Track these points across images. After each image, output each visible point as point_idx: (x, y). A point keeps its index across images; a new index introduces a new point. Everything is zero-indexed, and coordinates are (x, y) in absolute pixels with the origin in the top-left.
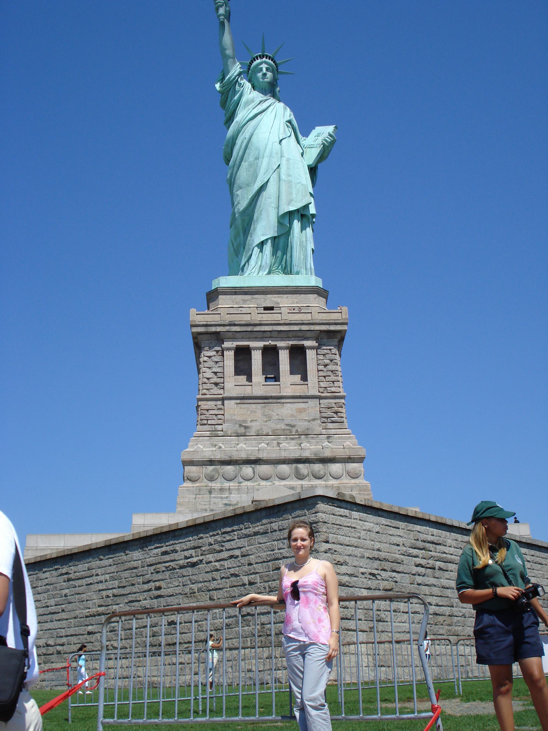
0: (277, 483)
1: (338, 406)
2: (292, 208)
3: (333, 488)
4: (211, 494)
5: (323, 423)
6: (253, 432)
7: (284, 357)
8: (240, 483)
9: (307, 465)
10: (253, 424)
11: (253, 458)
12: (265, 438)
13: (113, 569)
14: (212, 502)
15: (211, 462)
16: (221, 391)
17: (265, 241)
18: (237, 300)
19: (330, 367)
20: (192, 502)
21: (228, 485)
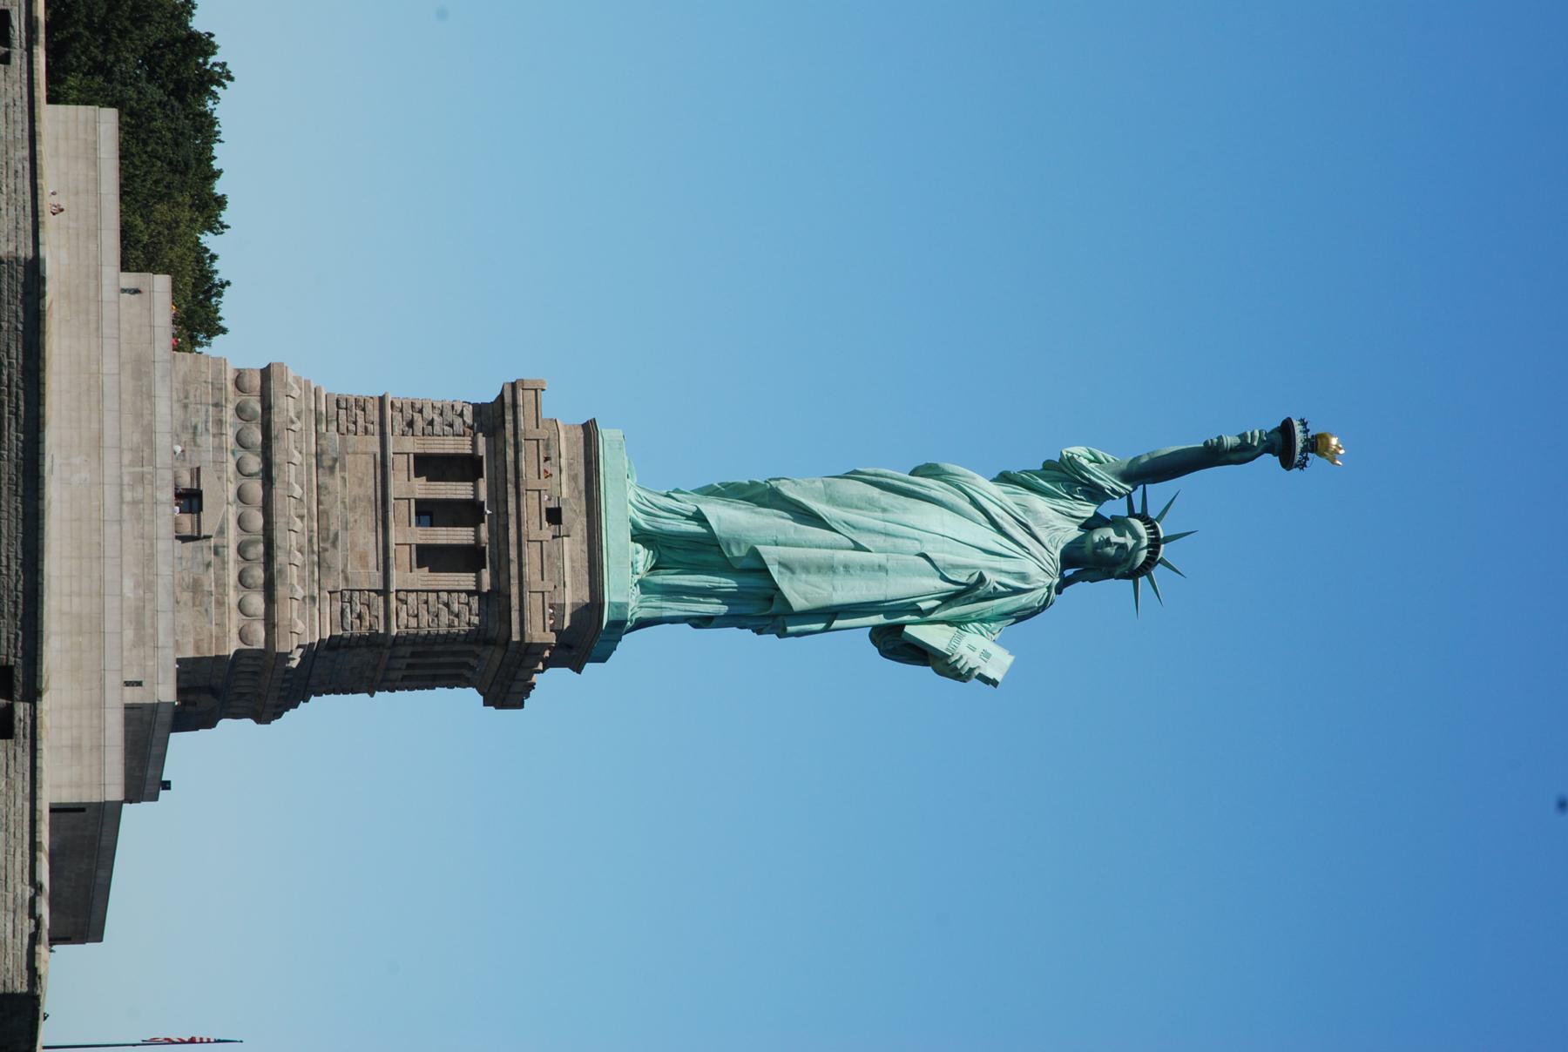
0: (232, 513)
1: (372, 622)
2: (774, 570)
3: (222, 595)
5: (342, 594)
7: (461, 536)
8: (233, 453)
9: (262, 560)
10: (339, 481)
11: (275, 472)
12: (312, 497)
13: (10, 138)
14: (199, 406)
15: (267, 408)
16: (397, 431)
17: (705, 524)
18: (576, 464)
20: (200, 376)
21: (230, 433)
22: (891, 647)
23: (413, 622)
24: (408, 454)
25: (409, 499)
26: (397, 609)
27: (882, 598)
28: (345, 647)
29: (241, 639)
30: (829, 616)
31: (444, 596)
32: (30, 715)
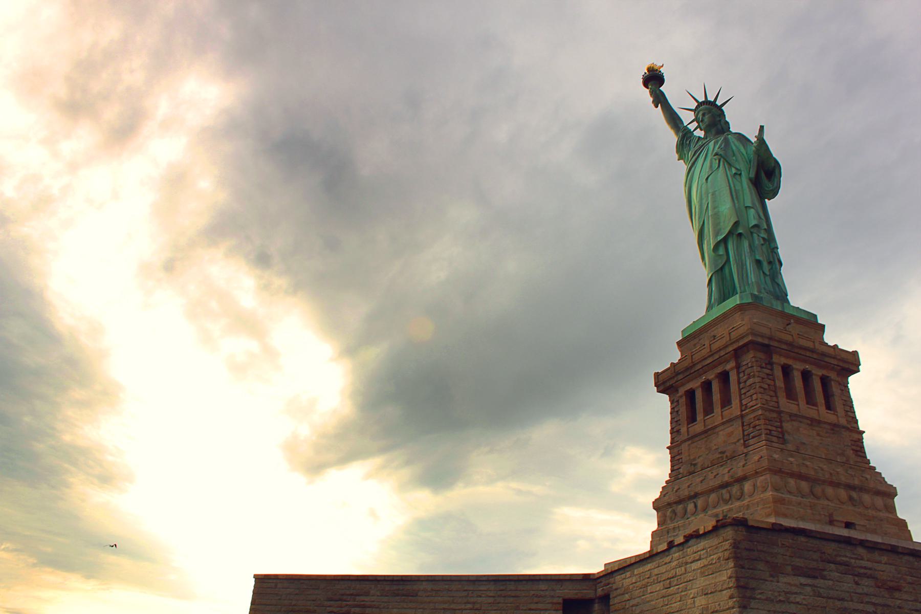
2: (720, 238)
4: (668, 534)
6: (699, 467)
7: (715, 387)
8: (688, 519)
9: (729, 488)
10: (699, 460)
11: (692, 494)
15: (669, 504)
19: (749, 383)
22: (770, 185)
23: (754, 397)
24: (688, 428)
25: (704, 421)
26: (749, 408)
27: (728, 188)
28: (783, 435)
29: (766, 490)
30: (748, 209)
31: (742, 386)
32: (601, 582)
